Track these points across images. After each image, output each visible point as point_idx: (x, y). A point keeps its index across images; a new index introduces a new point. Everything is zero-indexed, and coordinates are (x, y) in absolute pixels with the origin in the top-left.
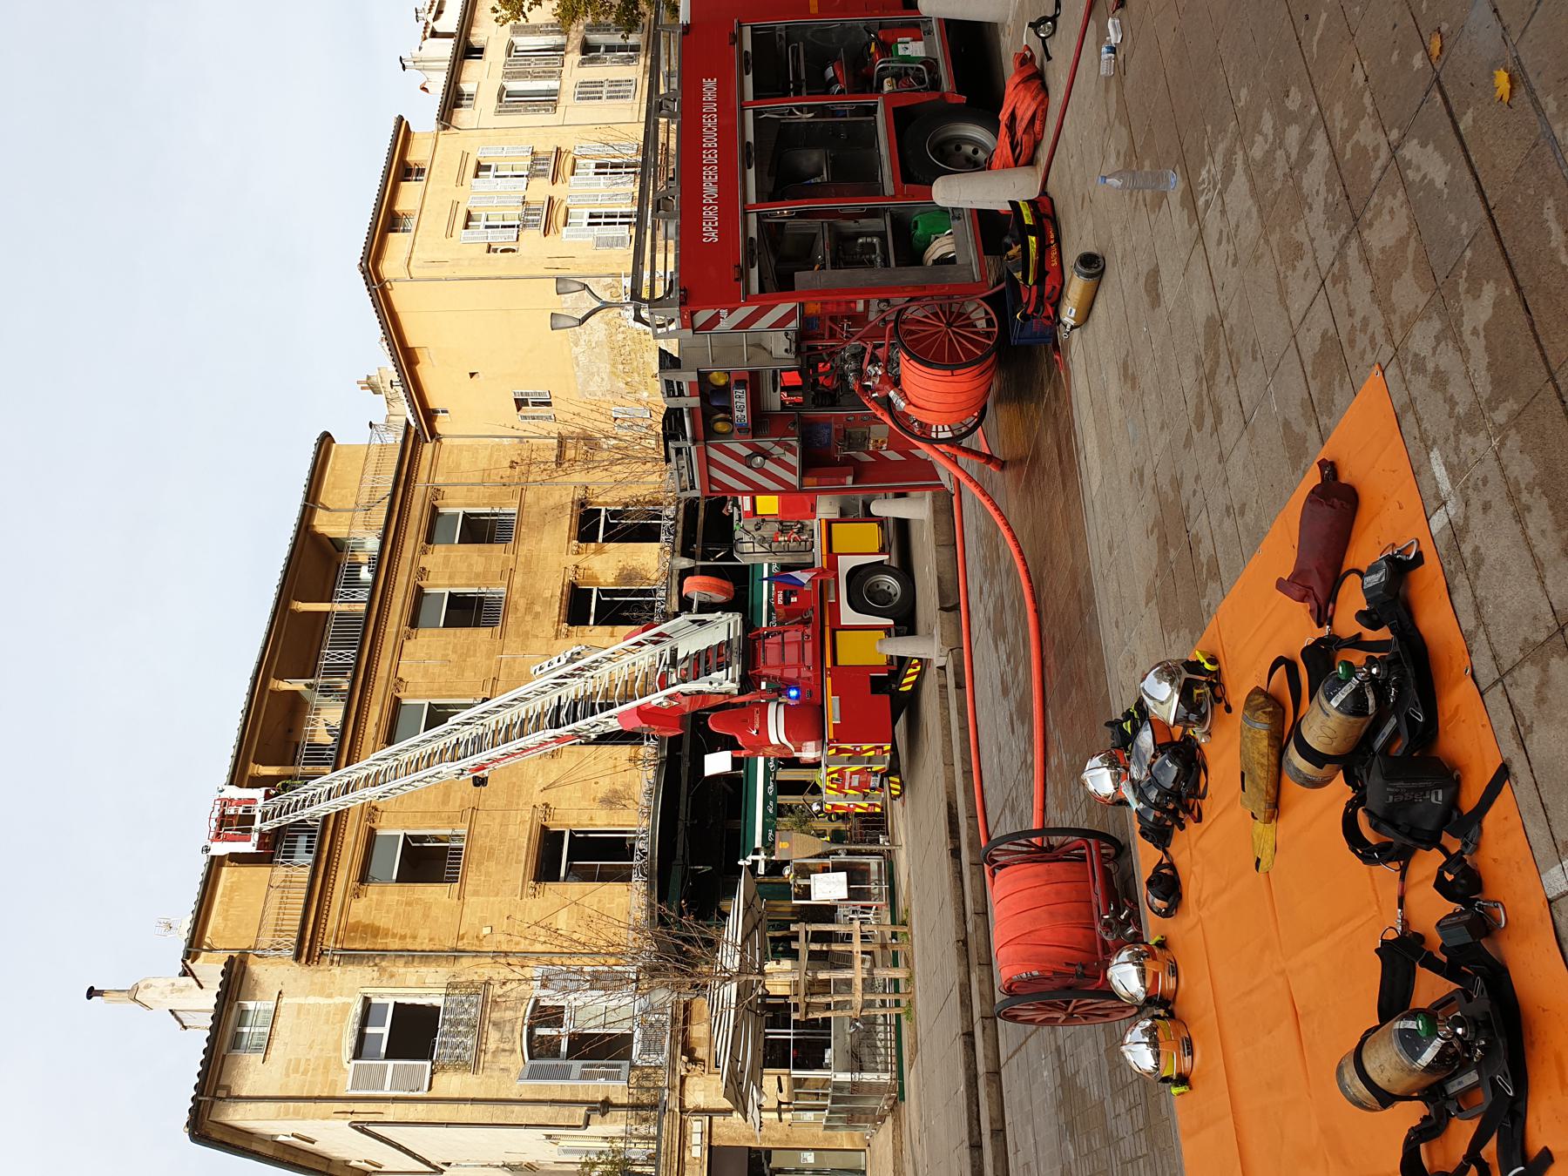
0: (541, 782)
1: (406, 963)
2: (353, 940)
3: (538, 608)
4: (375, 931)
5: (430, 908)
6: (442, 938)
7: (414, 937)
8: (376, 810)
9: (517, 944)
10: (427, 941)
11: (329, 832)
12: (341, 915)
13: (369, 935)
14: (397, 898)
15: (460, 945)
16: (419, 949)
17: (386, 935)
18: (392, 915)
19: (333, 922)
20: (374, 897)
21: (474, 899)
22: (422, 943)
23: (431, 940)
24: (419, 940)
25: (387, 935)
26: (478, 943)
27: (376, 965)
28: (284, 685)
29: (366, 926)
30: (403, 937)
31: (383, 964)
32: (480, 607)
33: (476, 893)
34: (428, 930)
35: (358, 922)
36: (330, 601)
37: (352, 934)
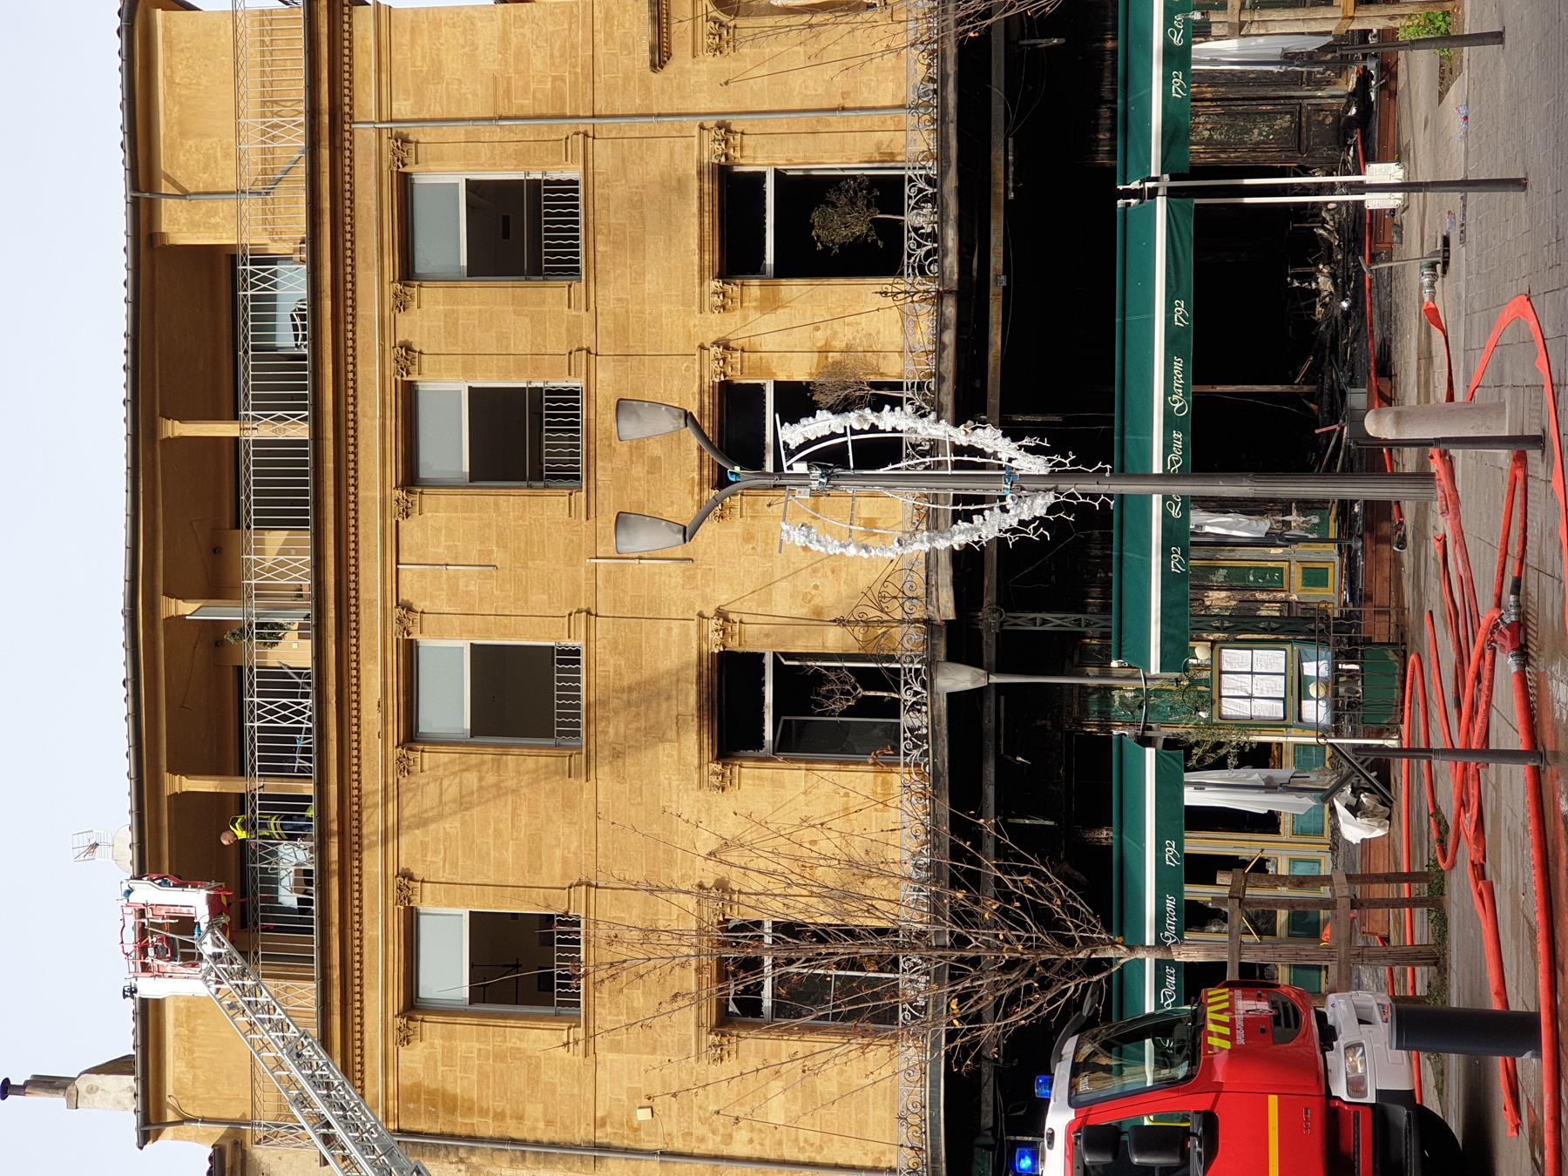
0: (707, 842)
1: (512, 1161)
2: (415, 1114)
3: (656, 450)
4: (450, 1104)
5: (537, 1067)
6: (568, 1123)
7: (520, 1118)
8: (411, 878)
9: (702, 1140)
10: (541, 1125)
11: (335, 931)
12: (386, 1075)
13: (440, 1108)
14: (477, 1045)
15: (602, 1137)
16: (530, 1137)
17: (469, 1110)
18: (474, 1077)
19: (374, 1082)
20: (438, 1042)
21: (610, 1056)
22: (534, 1129)
23: (549, 1123)
24: (528, 1123)
25: (470, 1109)
26: (632, 1136)
27: (461, 1161)
28: (187, 608)
29: (431, 1093)
30: (499, 1116)
31: (474, 1159)
32: (537, 414)
33: (616, 1047)
34: (540, 1107)
35: (418, 1085)
36: (236, 417)
37: (411, 1106)
